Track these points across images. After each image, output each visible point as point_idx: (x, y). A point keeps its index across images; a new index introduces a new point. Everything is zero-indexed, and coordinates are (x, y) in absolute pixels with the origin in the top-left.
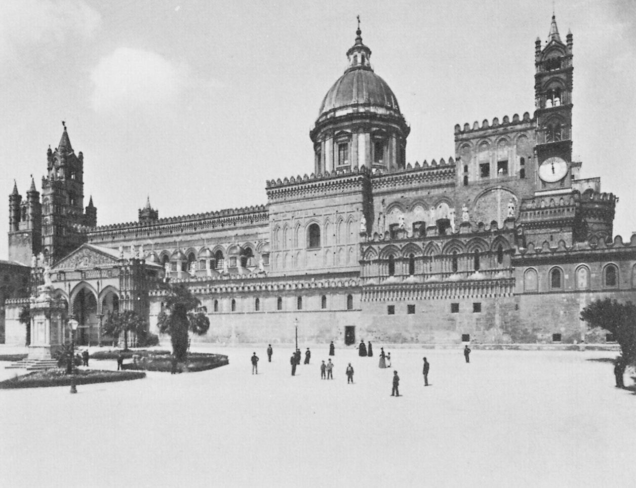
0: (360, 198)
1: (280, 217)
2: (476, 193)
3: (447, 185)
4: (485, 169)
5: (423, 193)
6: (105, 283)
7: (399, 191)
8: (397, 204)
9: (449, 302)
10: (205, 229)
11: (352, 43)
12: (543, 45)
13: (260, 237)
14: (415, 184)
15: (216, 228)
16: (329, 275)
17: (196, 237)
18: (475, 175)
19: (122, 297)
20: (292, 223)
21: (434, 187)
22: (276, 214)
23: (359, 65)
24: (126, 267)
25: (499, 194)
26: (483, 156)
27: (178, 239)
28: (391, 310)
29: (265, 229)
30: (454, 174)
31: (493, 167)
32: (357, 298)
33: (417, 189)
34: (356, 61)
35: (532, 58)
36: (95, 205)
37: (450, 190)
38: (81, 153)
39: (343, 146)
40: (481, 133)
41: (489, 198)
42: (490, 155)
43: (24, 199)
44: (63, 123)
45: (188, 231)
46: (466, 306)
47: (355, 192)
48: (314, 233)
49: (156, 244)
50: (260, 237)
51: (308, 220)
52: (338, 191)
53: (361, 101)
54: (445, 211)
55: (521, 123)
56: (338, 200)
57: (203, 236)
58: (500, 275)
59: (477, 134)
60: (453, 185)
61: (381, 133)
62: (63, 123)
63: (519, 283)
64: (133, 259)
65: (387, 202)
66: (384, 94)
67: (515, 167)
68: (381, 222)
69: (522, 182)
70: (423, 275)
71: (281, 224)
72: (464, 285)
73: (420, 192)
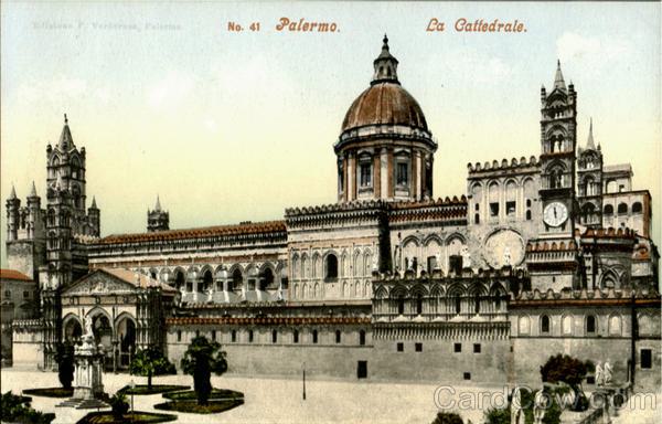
0: (376, 232)
1: (297, 246)
2: (487, 232)
4: (495, 207)
6: (121, 310)
7: (414, 226)
8: (412, 238)
10: (222, 247)
11: (377, 53)
12: (549, 91)
13: (280, 257)
14: (429, 220)
18: (485, 212)
19: (139, 324)
21: (447, 224)
22: (294, 243)
24: (143, 295)
27: (193, 256)
29: (284, 250)
30: (465, 212)
31: (502, 208)
32: (369, 337)
35: (539, 105)
36: (98, 207)
37: (461, 228)
38: (83, 148)
40: (491, 174)
42: (500, 194)
43: (24, 204)
45: (206, 248)
47: (371, 227)
49: (170, 260)
50: (280, 257)
52: (355, 225)
53: (384, 121)
55: (528, 166)
57: (221, 254)
58: (498, 319)
59: (488, 174)
60: (465, 223)
61: (407, 154)
64: (151, 287)
65: (403, 237)
66: (411, 113)
67: (521, 209)
68: (398, 255)
69: (529, 223)
70: (430, 315)
71: (299, 253)
72: (467, 328)
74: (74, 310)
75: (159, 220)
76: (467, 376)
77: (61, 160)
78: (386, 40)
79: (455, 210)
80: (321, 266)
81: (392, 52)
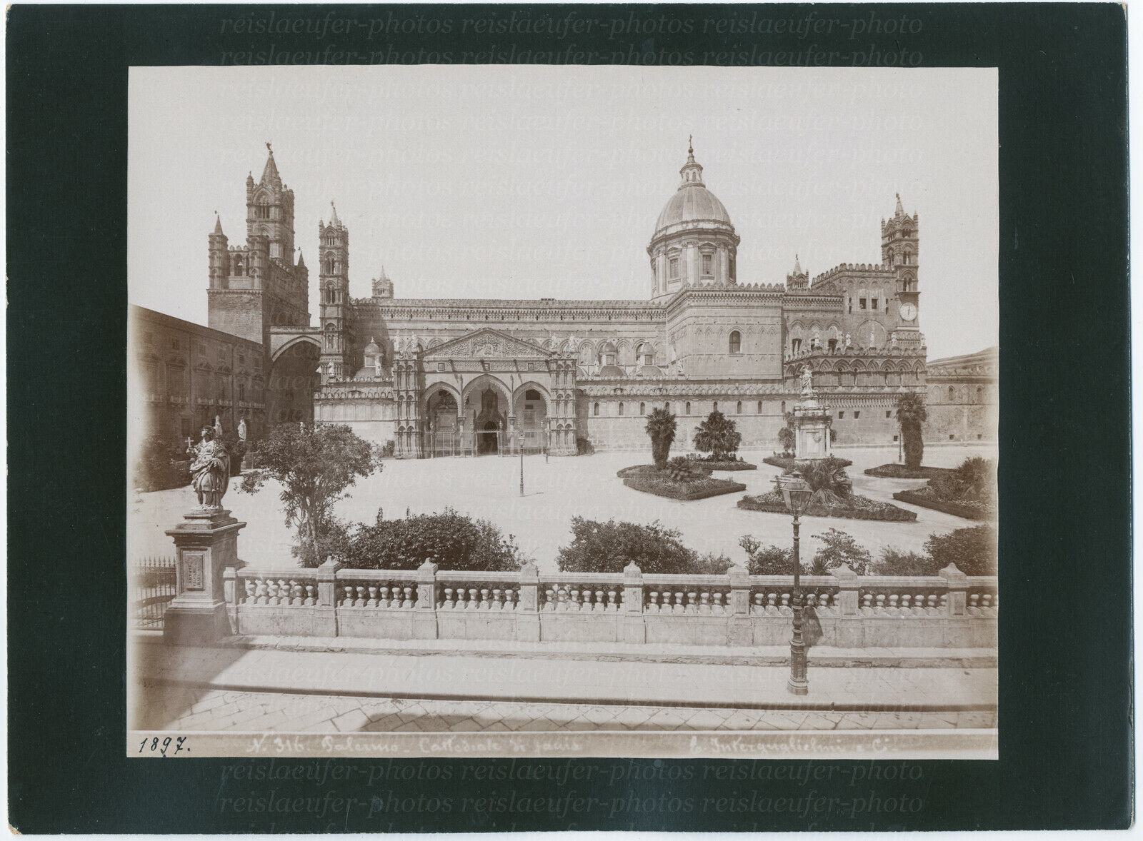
4: (863, 301)
15: (566, 320)
18: (857, 307)
23: (690, 182)
26: (861, 293)
30: (841, 302)
31: (869, 304)
33: (814, 311)
37: (838, 315)
44: (268, 145)
48: (735, 338)
51: (730, 327)
60: (842, 312)
62: (268, 145)
71: (704, 328)
73: (816, 314)
80: (726, 339)
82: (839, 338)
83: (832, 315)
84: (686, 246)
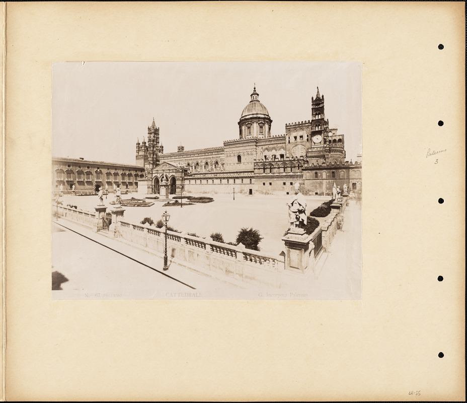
1: (228, 153)
2: (293, 146)
3: (283, 143)
4: (296, 138)
5: (276, 145)
6: (171, 174)
8: (267, 149)
9: (282, 182)
14: (272, 143)
16: (244, 172)
17: (199, 157)
18: (292, 140)
20: (232, 155)
25: (300, 146)
26: (294, 134)
28: (264, 184)
31: (298, 138)
34: (254, 99)
37: (284, 145)
39: (249, 128)
41: (296, 147)
43: (141, 144)
46: (288, 183)
47: (253, 145)
48: (239, 158)
54: (282, 152)
56: (247, 148)
57: (202, 157)
58: (299, 174)
60: (285, 143)
63: (304, 177)
67: (305, 138)
74: (156, 174)
75: (181, 149)
76: (288, 193)
77: (153, 131)
78: (255, 88)
79: (283, 138)
80: (236, 158)
81: (257, 92)
82: (284, 154)
83: (281, 145)
84: (254, 123)
